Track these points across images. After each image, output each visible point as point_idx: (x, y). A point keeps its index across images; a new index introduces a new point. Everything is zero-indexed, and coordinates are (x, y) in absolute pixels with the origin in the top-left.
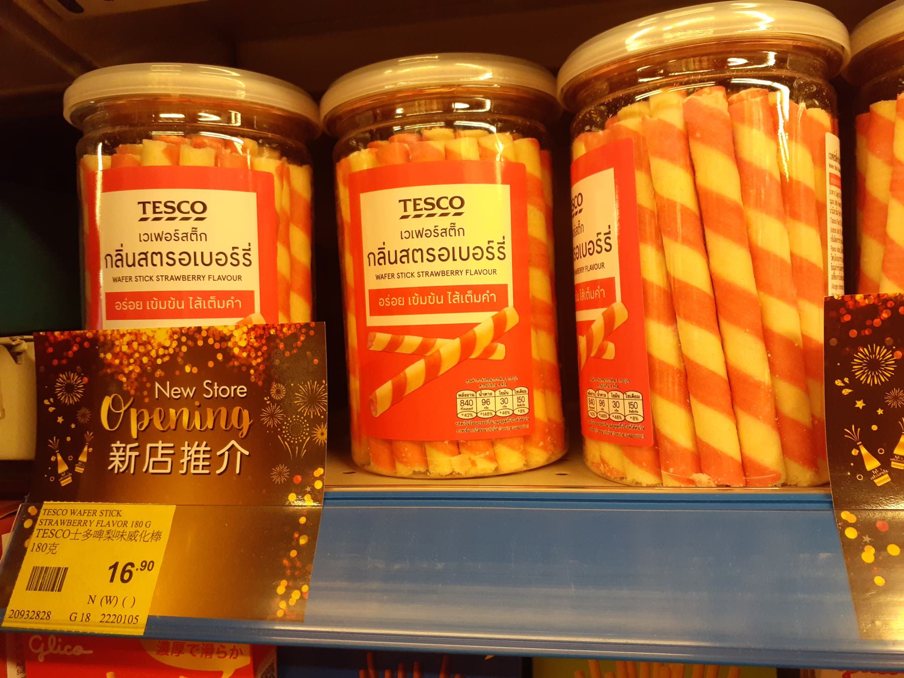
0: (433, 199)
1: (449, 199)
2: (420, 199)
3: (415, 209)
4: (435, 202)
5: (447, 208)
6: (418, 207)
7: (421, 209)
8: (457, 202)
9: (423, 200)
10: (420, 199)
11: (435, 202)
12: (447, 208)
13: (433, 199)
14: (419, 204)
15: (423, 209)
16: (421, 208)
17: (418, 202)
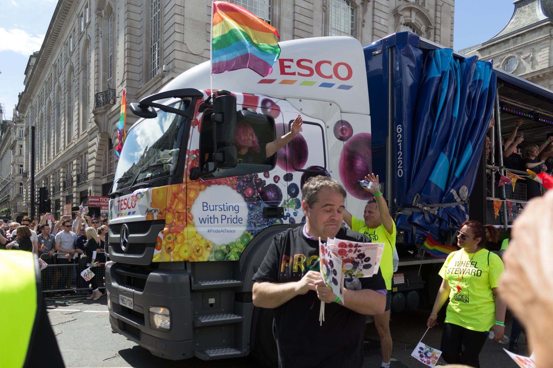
0: (311, 61)
1: (333, 64)
2: (292, 60)
3: (283, 72)
4: (313, 66)
5: (331, 77)
6: (287, 70)
7: (294, 74)
8: (343, 71)
9: (295, 61)
10: (292, 60)
11: (313, 66)
12: (331, 77)
13: (311, 61)
14: (289, 67)
15: (297, 74)
16: (294, 72)
17: (286, 63)
